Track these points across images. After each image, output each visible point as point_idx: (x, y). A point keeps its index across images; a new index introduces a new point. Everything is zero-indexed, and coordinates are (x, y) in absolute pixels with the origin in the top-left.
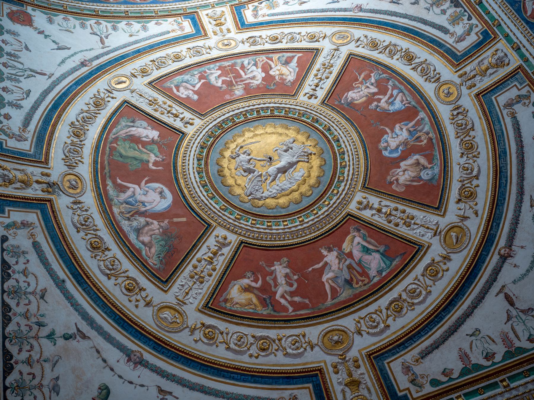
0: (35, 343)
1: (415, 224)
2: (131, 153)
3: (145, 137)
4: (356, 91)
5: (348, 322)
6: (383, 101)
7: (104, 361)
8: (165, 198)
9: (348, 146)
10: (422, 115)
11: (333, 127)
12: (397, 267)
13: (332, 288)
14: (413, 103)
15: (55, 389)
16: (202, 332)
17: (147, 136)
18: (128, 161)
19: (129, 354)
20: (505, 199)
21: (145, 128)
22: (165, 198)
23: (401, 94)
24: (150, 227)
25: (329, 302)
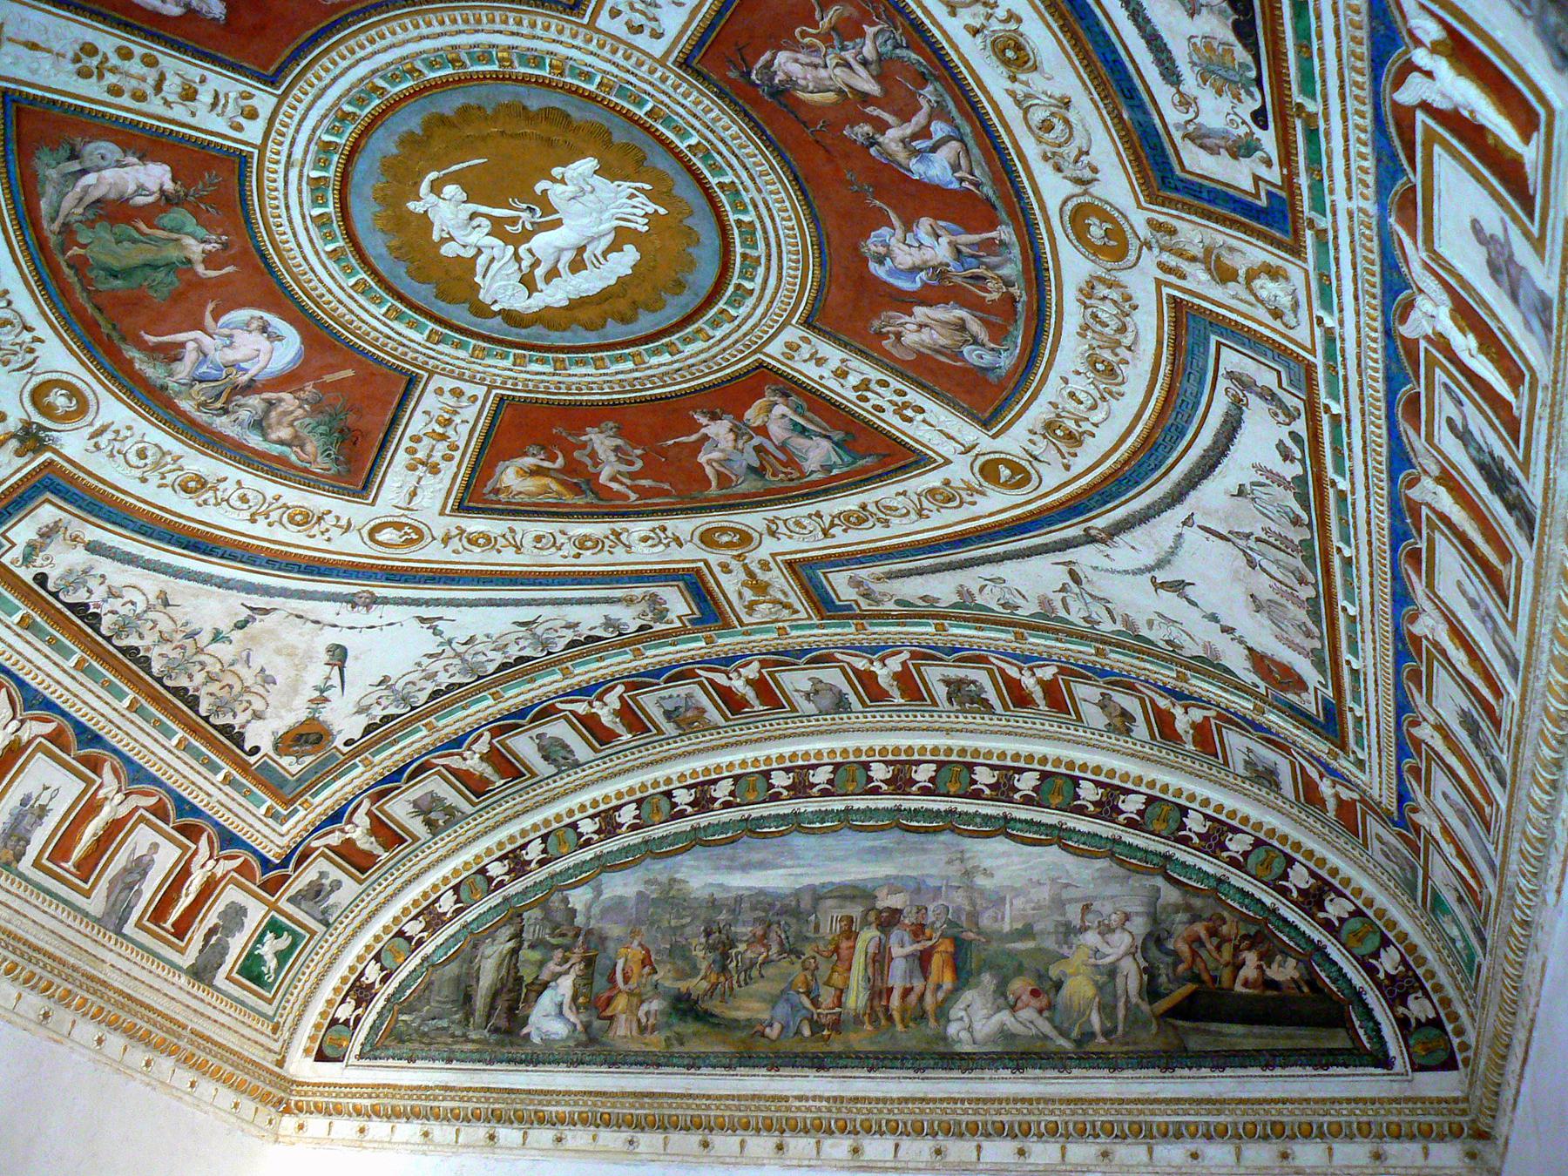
0: (202, 658)
1: (924, 421)
2: (132, 255)
3: (136, 193)
4: (802, 57)
5: (753, 520)
6: (891, 133)
7: (317, 622)
8: (280, 338)
9: (767, 221)
10: (1005, 233)
11: (720, 153)
12: (864, 470)
13: (719, 474)
14: (988, 190)
15: (269, 680)
16: (465, 541)
17: (141, 189)
18: (138, 277)
19: (352, 601)
20: (1137, 483)
21: (119, 164)
22: (280, 338)
23: (955, 144)
24: (280, 409)
25: (714, 490)
